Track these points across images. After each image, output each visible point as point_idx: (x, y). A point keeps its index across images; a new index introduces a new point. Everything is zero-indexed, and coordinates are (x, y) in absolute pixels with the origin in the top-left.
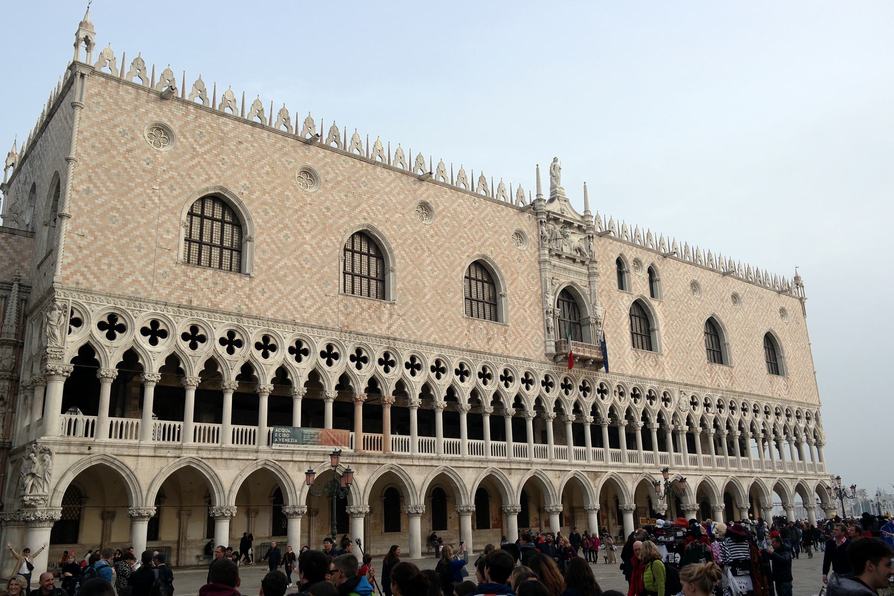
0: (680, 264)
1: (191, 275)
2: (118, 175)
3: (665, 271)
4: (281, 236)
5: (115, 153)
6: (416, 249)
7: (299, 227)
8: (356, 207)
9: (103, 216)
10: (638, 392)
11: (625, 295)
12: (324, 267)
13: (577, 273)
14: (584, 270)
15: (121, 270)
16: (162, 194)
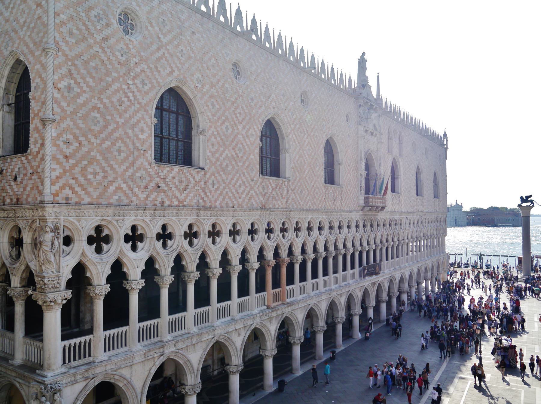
1: (162, 175)
2: (96, 68)
4: (223, 128)
5: (92, 41)
6: (301, 132)
7: (235, 119)
8: (269, 97)
9: (84, 118)
12: (250, 154)
15: (105, 177)
16: (135, 90)
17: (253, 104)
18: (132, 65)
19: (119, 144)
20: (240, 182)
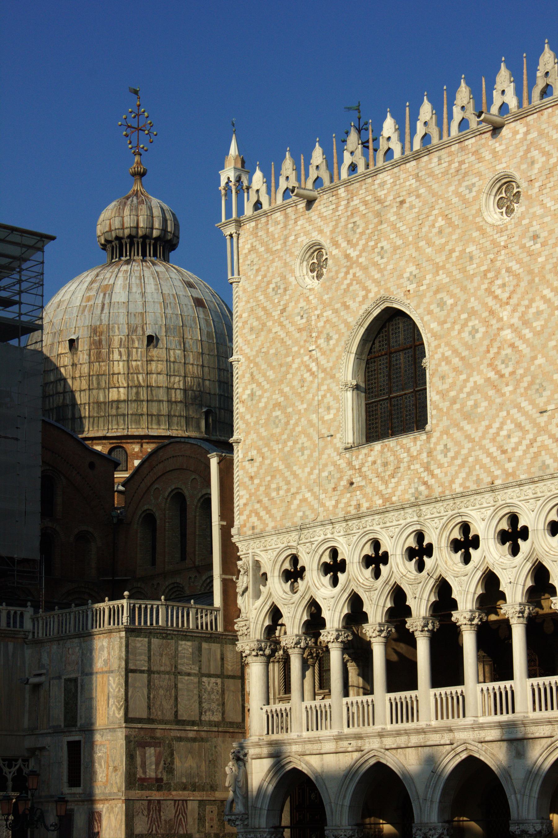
1: (356, 464)
2: (276, 354)
4: (465, 335)
12: (534, 358)
15: (288, 490)
17: (538, 246)
18: (313, 323)
19: (303, 439)
20: (509, 426)
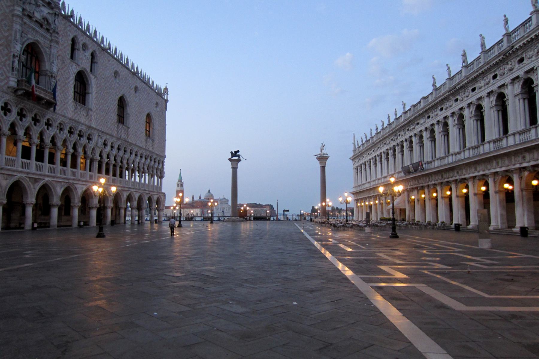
0: (110, 58)
3: (101, 58)
10: (72, 130)
11: (74, 65)
13: (42, 36)
14: (48, 36)
